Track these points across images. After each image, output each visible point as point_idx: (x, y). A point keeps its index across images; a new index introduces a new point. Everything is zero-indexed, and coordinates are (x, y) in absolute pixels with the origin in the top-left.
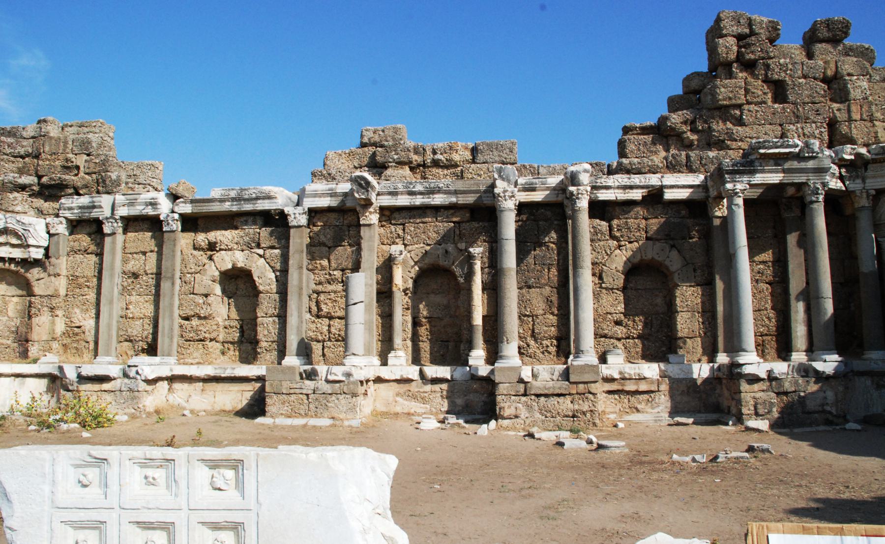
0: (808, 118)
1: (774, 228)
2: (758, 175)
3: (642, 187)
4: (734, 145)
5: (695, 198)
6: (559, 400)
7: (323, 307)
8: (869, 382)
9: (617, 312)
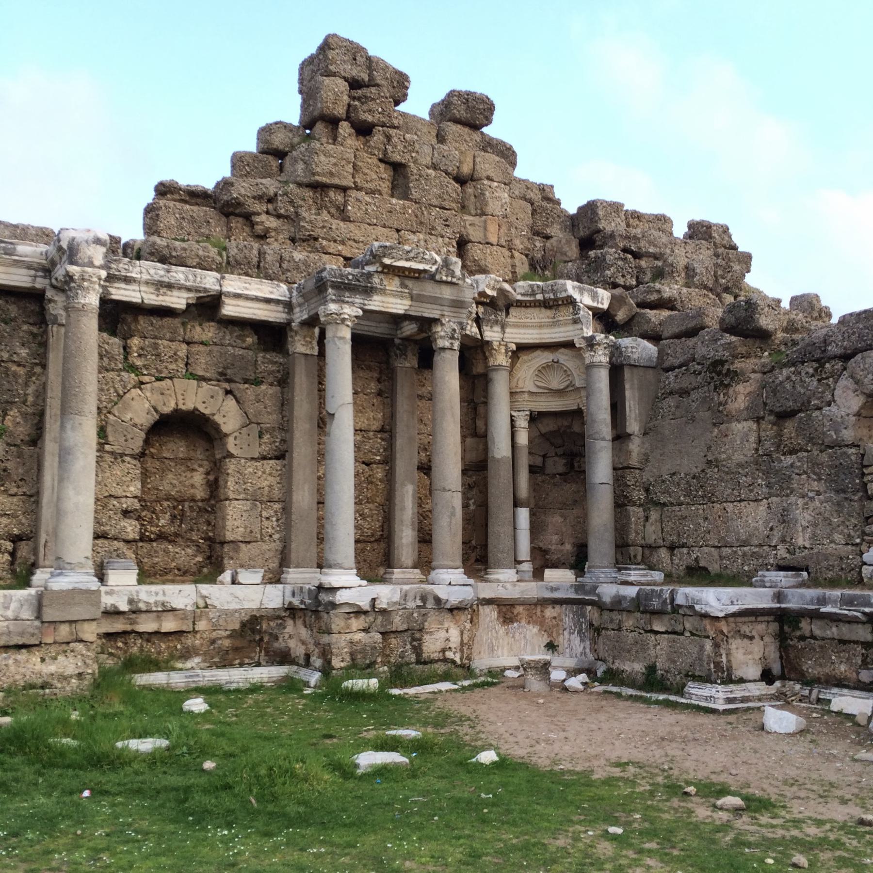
0: (433, 228)
1: (379, 381)
2: (375, 297)
3: (189, 289)
4: (333, 248)
5: (270, 320)
6: (19, 657)
8: (495, 614)
9: (129, 495)
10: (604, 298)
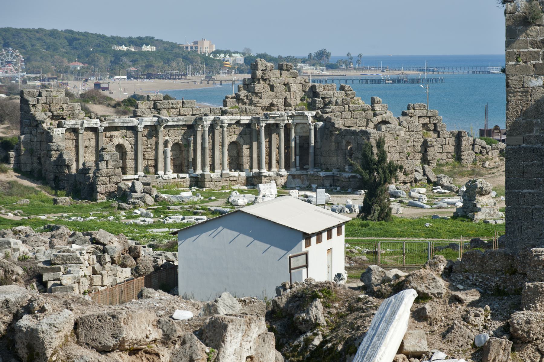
7: (146, 156)
10: (314, 113)
